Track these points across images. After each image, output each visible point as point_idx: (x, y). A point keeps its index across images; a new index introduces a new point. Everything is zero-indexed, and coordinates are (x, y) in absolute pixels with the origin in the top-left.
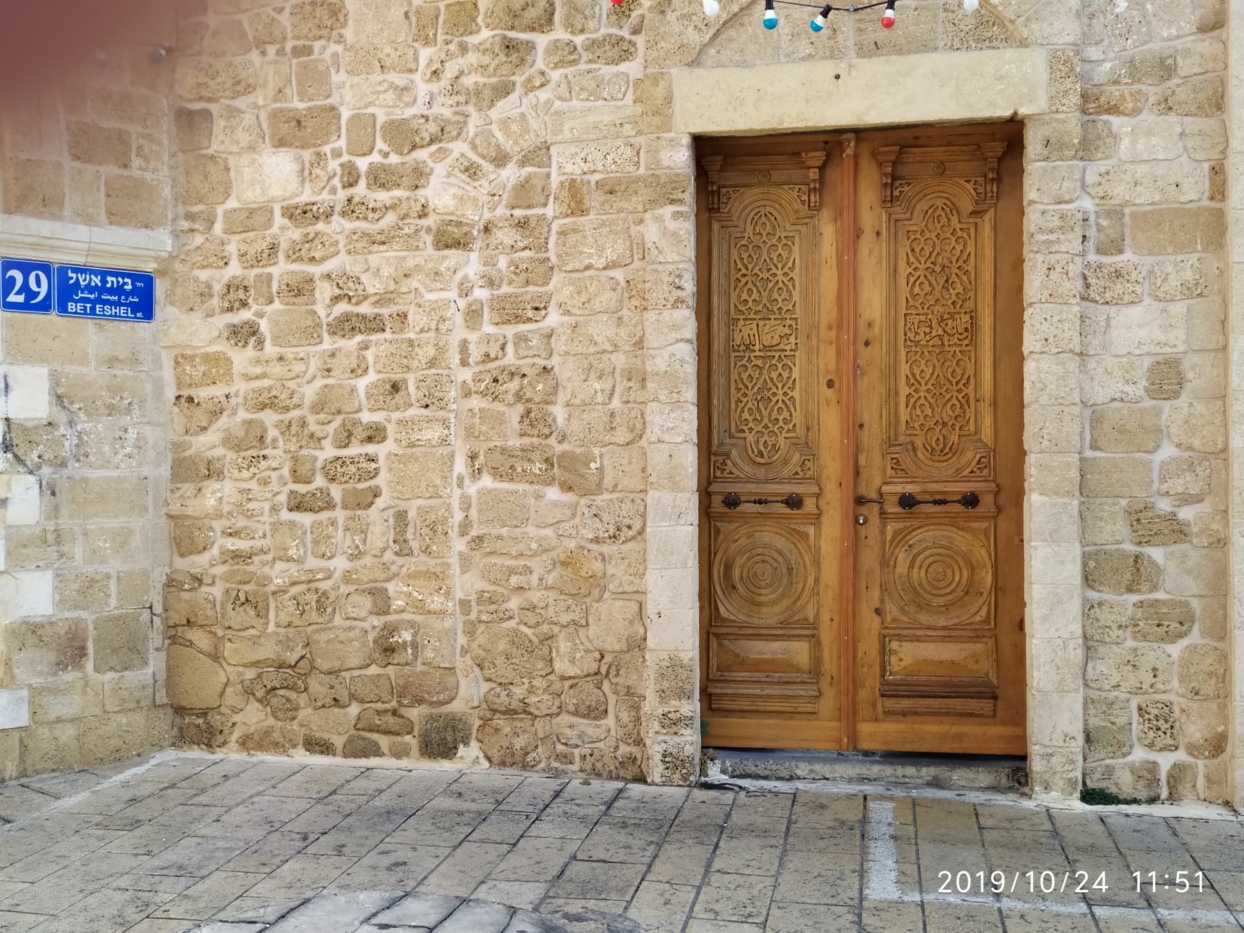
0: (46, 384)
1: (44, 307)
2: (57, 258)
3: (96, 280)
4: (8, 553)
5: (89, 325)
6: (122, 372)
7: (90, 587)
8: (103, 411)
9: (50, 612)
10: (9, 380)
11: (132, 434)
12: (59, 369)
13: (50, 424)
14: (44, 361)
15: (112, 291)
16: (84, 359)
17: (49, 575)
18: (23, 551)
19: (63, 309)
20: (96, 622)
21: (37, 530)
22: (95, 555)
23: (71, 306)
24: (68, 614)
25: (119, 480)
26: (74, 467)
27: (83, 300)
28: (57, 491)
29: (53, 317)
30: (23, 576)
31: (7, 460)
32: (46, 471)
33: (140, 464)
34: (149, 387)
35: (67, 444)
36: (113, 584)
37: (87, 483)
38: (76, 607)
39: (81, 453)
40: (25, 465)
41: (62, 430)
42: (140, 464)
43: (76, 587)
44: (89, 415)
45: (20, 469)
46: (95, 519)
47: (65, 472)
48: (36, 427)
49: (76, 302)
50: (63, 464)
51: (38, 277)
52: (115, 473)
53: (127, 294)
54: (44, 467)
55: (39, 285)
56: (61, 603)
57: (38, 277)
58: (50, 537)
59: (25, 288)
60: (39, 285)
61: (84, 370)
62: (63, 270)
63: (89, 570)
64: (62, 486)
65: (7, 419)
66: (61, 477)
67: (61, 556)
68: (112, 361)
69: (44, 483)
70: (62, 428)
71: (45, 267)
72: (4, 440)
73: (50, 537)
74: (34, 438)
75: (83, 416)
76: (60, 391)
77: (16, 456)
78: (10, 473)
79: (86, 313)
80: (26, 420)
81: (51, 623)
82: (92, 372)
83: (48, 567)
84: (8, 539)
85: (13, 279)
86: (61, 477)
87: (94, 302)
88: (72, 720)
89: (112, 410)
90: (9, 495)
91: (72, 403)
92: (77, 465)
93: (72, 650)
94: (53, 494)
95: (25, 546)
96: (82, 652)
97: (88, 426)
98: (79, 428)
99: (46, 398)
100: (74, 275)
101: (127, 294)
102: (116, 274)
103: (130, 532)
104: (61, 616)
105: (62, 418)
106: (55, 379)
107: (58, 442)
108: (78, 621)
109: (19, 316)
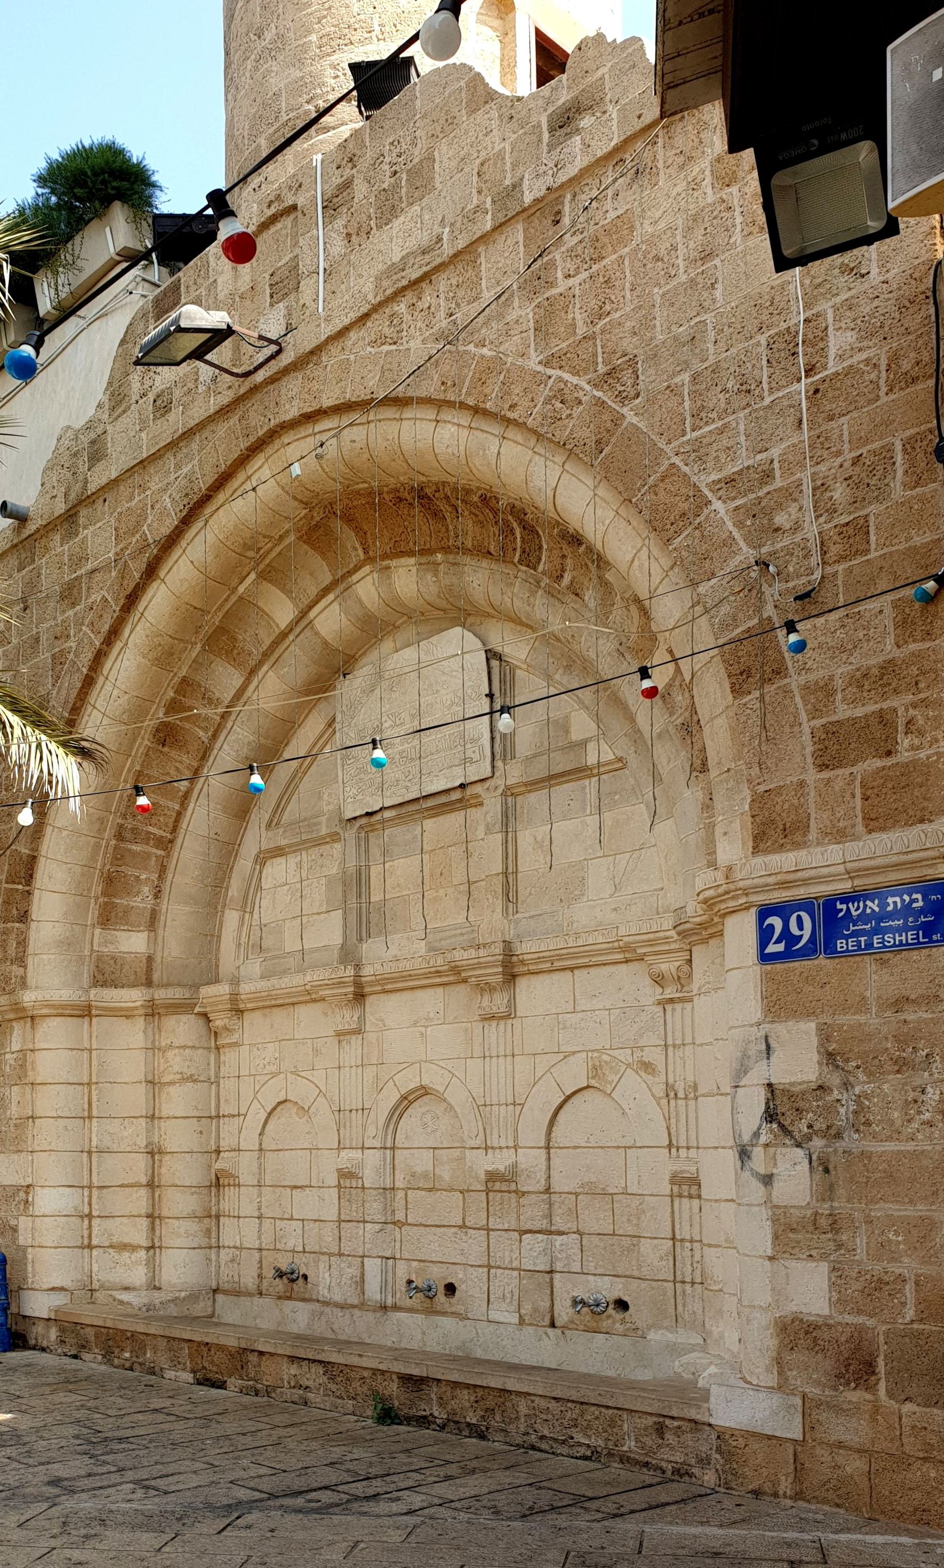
0: (815, 1041)
1: (810, 951)
4: (776, 1237)
7: (879, 1288)
8: (888, 1066)
9: (826, 1312)
10: (771, 1041)
12: (829, 1021)
13: (820, 1087)
14: (810, 1014)
17: (824, 1267)
18: (791, 1235)
20: (887, 1333)
21: (809, 1213)
23: (840, 944)
24: (849, 1319)
27: (856, 934)
28: (831, 1167)
29: (821, 960)
30: (793, 1264)
31: (771, 1131)
35: (842, 1111)
36: (909, 1289)
37: (870, 1158)
38: (860, 1312)
39: (861, 1121)
40: (792, 1137)
41: (836, 1094)
43: (858, 1286)
44: (870, 1074)
45: (787, 1142)
46: (882, 1204)
47: (840, 1145)
48: (803, 1093)
49: (847, 938)
50: (838, 1136)
51: (799, 919)
54: (815, 1138)
55: (801, 926)
56: (841, 1302)
57: (799, 919)
58: (823, 1222)
60: (801, 926)
61: (862, 1018)
62: (830, 904)
63: (877, 1268)
65: (770, 1085)
66: (836, 1151)
67: (840, 1246)
69: (814, 1157)
70: (836, 1092)
71: (806, 905)
72: (768, 1108)
73: (823, 1222)
74: (801, 1104)
75: (862, 1077)
76: (832, 1047)
77: (782, 1126)
78: (776, 1145)
79: (860, 949)
80: (791, 1084)
81: (830, 1327)
82: (871, 1020)
83: (824, 1257)
84: (775, 1221)
85: (772, 927)
86: (836, 1151)
88: (859, 1451)
89: (901, 1065)
90: (775, 1171)
91: (847, 1060)
92: (856, 1136)
94: (827, 1170)
95: (792, 1230)
96: (870, 1367)
97: (868, 1088)
98: (857, 1090)
99: (816, 1057)
100: (844, 907)
104: (839, 1318)
105: (835, 1079)
107: (831, 1109)
108: (861, 1330)
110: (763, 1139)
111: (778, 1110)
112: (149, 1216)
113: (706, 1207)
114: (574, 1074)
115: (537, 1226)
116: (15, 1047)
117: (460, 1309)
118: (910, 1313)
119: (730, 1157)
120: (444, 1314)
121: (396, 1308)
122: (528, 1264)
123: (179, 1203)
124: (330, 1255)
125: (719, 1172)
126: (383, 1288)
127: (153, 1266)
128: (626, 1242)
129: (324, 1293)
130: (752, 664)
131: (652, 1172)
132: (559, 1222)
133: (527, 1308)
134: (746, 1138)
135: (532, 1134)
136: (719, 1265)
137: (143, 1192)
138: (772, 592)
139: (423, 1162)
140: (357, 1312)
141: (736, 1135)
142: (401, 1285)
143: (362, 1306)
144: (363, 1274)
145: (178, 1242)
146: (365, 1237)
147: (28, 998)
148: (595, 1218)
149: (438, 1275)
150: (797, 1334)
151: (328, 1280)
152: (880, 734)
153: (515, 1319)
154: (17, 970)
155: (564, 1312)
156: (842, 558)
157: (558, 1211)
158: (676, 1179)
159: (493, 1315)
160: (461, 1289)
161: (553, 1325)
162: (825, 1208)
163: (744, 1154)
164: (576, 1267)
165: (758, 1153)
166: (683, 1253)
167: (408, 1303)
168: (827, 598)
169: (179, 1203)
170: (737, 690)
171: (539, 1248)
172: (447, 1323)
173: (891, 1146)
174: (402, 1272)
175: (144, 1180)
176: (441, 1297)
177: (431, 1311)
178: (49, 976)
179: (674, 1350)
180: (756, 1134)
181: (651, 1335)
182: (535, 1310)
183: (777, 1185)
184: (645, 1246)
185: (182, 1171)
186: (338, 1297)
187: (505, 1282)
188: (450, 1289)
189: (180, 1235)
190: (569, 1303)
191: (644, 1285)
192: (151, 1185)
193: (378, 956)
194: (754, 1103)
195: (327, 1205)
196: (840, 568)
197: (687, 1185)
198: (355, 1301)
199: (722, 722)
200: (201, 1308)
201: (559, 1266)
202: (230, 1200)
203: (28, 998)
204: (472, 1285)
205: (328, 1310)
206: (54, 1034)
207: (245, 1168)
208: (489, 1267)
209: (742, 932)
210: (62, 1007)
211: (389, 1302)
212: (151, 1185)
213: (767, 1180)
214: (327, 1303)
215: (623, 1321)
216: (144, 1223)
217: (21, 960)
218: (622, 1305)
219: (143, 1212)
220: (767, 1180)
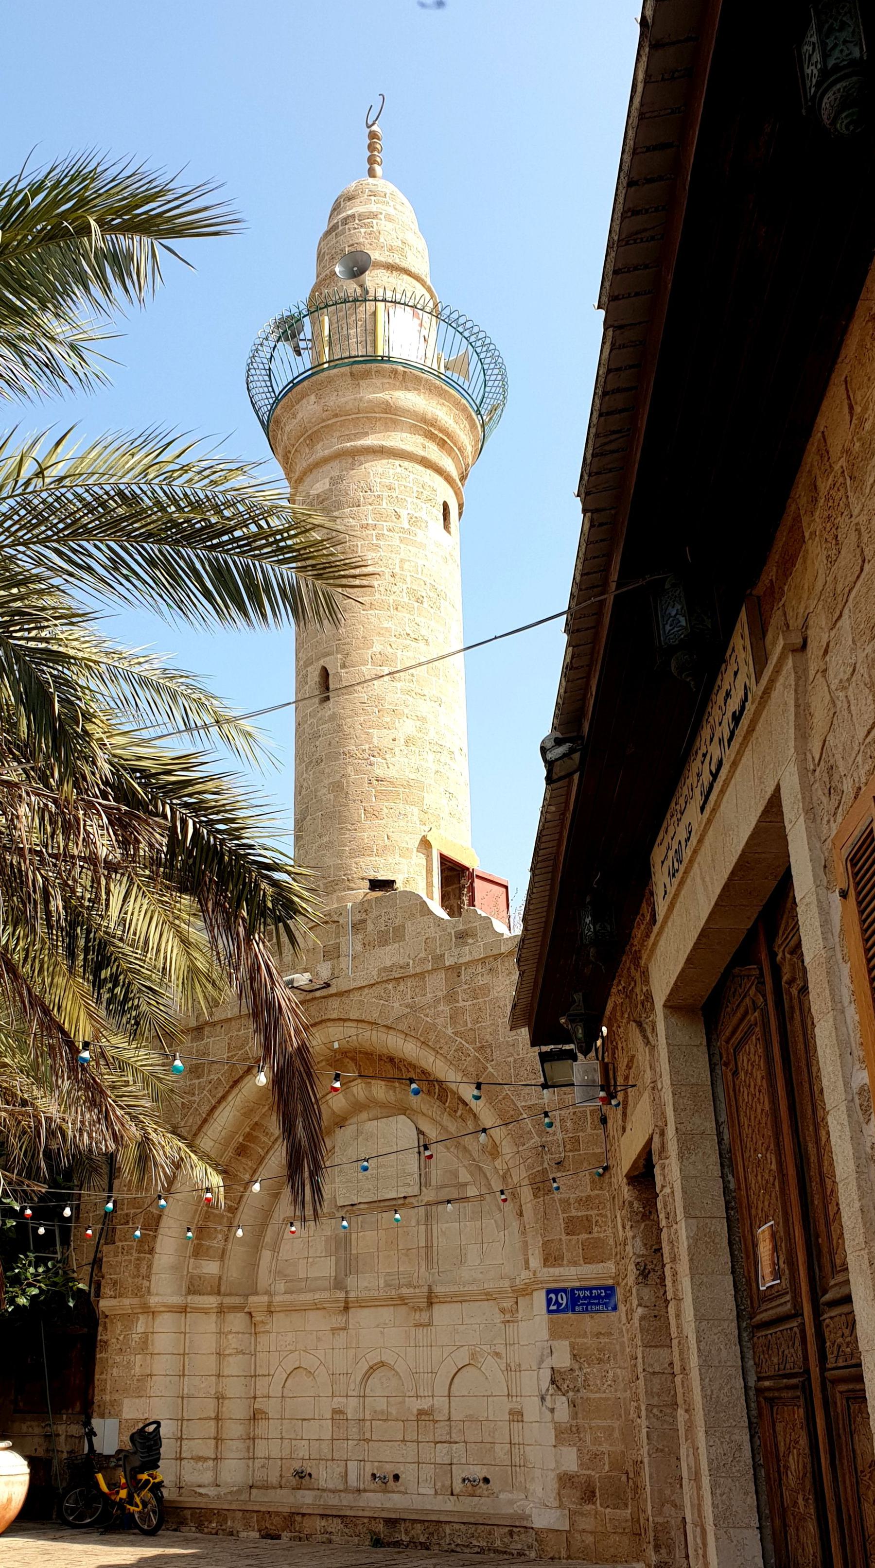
2: (568, 1285)
3: (588, 1293)
5: (587, 1316)
6: (604, 1340)
11: (611, 1374)
15: (595, 1298)
16: (585, 1336)
19: (573, 1310)
22: (596, 1441)
25: (607, 1399)
26: (583, 1393)
32: (571, 1394)
33: (616, 1391)
34: (618, 1347)
42: (616, 1391)
52: (603, 1396)
53: (603, 1298)
59: (557, 1302)
64: (578, 1401)
68: (598, 1335)
87: (587, 1305)
93: (589, 1495)
101: (603, 1298)
102: (596, 1288)
103: (613, 1429)
106: (572, 1347)
109: (555, 1316)
110: (550, 1392)
112: (215, 1438)
113: (525, 1425)
114: (462, 1357)
115: (444, 1439)
116: (140, 1330)
117: (402, 1489)
118: (607, 1468)
119: (537, 1400)
120: (393, 1492)
121: (365, 1491)
122: (439, 1461)
123: (234, 1430)
124: (327, 1460)
125: (532, 1408)
126: (358, 1479)
127: (216, 1469)
128: (488, 1446)
129: (322, 1484)
130: (542, 1185)
131: (499, 1409)
132: (455, 1437)
133: (439, 1485)
134: (544, 1392)
135: (441, 1389)
137: (213, 1423)
138: (547, 1157)
140: (343, 1495)
141: (540, 1390)
142: (368, 1477)
143: (346, 1490)
144: (346, 1471)
145: (232, 1455)
147: (153, 1300)
149: (389, 1469)
151: (325, 1476)
153: (432, 1492)
154: (146, 1283)
155: (458, 1487)
156: (571, 1151)
157: (454, 1431)
158: (511, 1413)
159: (421, 1491)
160: (402, 1476)
161: (452, 1494)
162: (574, 1423)
163: (543, 1399)
164: (464, 1461)
165: (548, 1398)
166: (515, 1451)
167: (373, 1486)
168: (566, 1164)
169: (234, 1430)
170: (535, 1196)
171: (445, 1451)
172: (396, 1497)
173: (597, 1395)
174: (369, 1469)
175: (213, 1415)
176: (391, 1483)
177: (385, 1491)
178: (164, 1288)
179: (511, 1502)
180: (548, 1390)
181: (501, 1496)
182: (443, 1486)
183: (556, 1413)
184: (498, 1447)
186: (331, 1486)
187: (428, 1471)
188: (396, 1477)
189: (234, 1449)
190: (460, 1481)
191: (497, 1468)
192: (217, 1419)
194: (546, 1375)
196: (571, 1154)
197: (517, 1416)
198: (341, 1487)
199: (529, 1205)
200: (244, 1496)
201: (455, 1461)
203: (153, 1300)
204: (408, 1474)
205: (325, 1494)
206: (165, 1324)
208: (419, 1463)
209: (540, 1298)
210: (173, 1307)
211: (362, 1487)
212: (217, 1419)
213: (552, 1410)
214: (324, 1490)
215: (487, 1489)
216: (213, 1442)
217: (148, 1277)
218: (486, 1480)
219: (212, 1436)
220: (552, 1410)
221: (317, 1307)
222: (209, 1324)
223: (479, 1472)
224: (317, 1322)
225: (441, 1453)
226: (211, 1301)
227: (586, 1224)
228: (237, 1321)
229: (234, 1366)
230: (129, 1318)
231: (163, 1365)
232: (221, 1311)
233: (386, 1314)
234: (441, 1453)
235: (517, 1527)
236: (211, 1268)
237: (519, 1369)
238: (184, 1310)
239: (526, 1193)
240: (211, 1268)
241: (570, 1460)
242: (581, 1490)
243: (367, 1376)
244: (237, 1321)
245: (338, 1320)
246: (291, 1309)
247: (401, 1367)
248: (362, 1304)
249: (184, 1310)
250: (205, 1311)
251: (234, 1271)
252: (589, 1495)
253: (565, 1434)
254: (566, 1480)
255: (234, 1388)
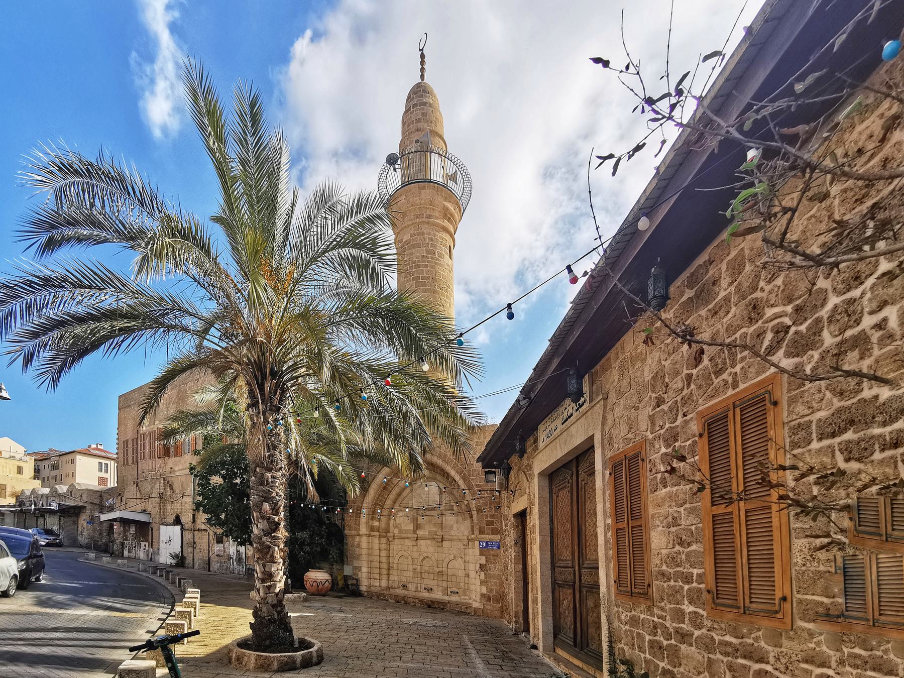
93: (489, 599)
111: (481, 566)
123: (384, 572)
125: (472, 574)
135: (445, 566)
136: (472, 587)
139: (427, 568)
146: (418, 580)
148: (454, 579)
150: (483, 595)
152: (492, 523)
169: (384, 572)
178: (363, 530)
185: (384, 566)
189: (384, 577)
193: (420, 533)
194: (478, 566)
195: (411, 574)
197: (468, 576)
202: (392, 572)
204: (435, 589)
207: (395, 566)
221: (408, 538)
222: (376, 540)
223: (456, 590)
224: (408, 543)
225: (445, 584)
226: (377, 534)
227: (492, 523)
228: (384, 540)
229: (384, 553)
230: (353, 536)
231: (364, 552)
232: (380, 537)
233: (429, 542)
234: (445, 584)
235: (468, 606)
236: (376, 524)
237: (468, 562)
238: (369, 536)
239: (474, 513)
240: (376, 524)
241: (484, 590)
242: (486, 598)
243: (423, 560)
244: (384, 540)
245: (414, 543)
246: (400, 538)
247: (433, 558)
248: (422, 539)
249: (369, 536)
250: (376, 537)
251: (383, 525)
252: (489, 599)
253: (482, 583)
254: (483, 595)
255: (384, 560)
